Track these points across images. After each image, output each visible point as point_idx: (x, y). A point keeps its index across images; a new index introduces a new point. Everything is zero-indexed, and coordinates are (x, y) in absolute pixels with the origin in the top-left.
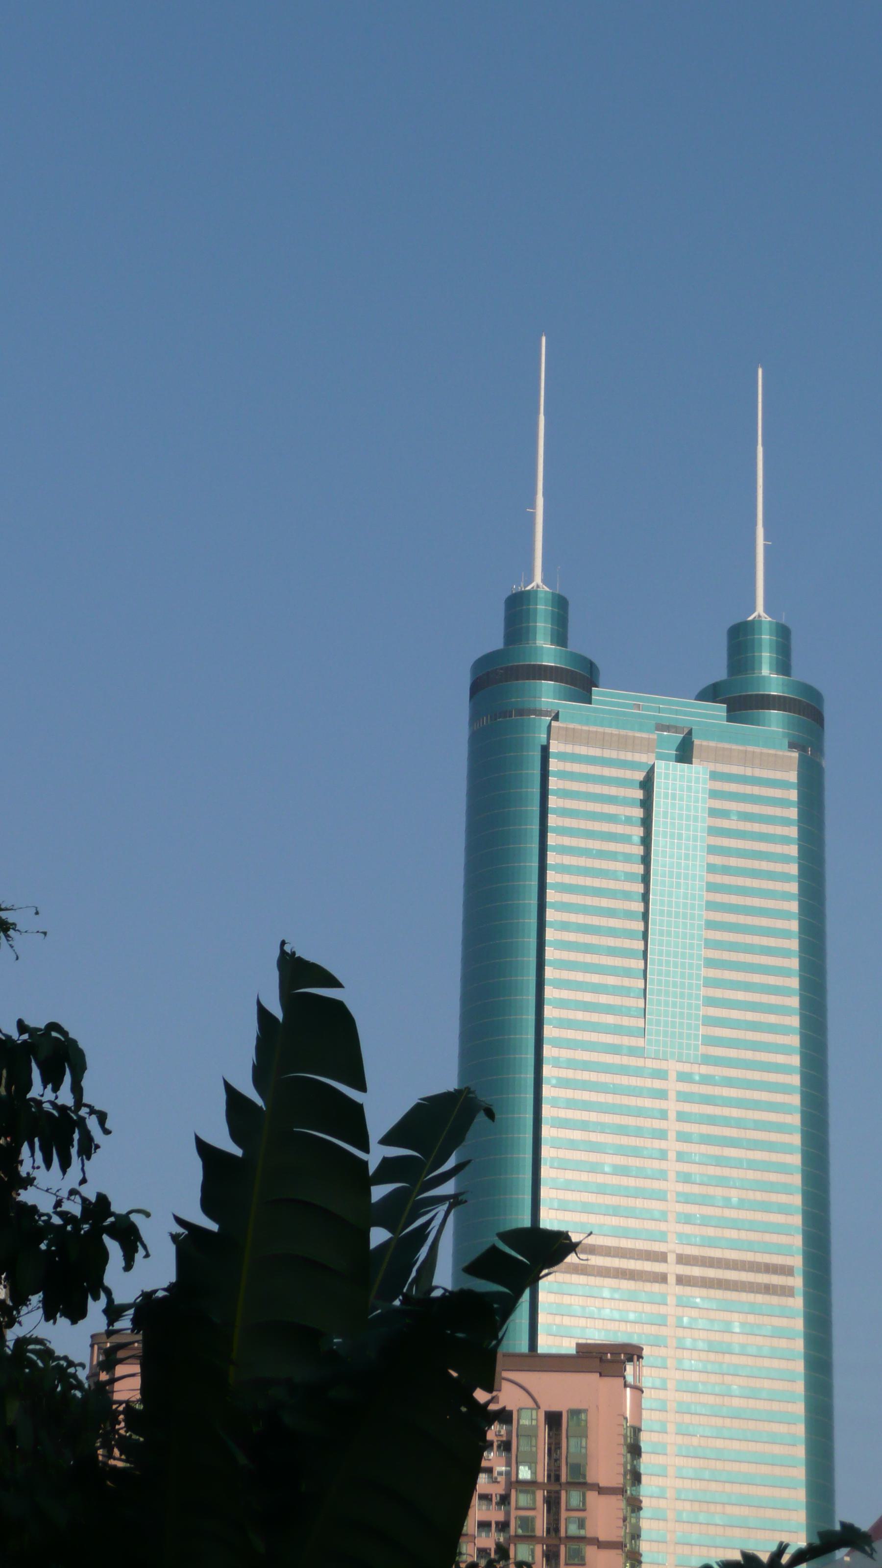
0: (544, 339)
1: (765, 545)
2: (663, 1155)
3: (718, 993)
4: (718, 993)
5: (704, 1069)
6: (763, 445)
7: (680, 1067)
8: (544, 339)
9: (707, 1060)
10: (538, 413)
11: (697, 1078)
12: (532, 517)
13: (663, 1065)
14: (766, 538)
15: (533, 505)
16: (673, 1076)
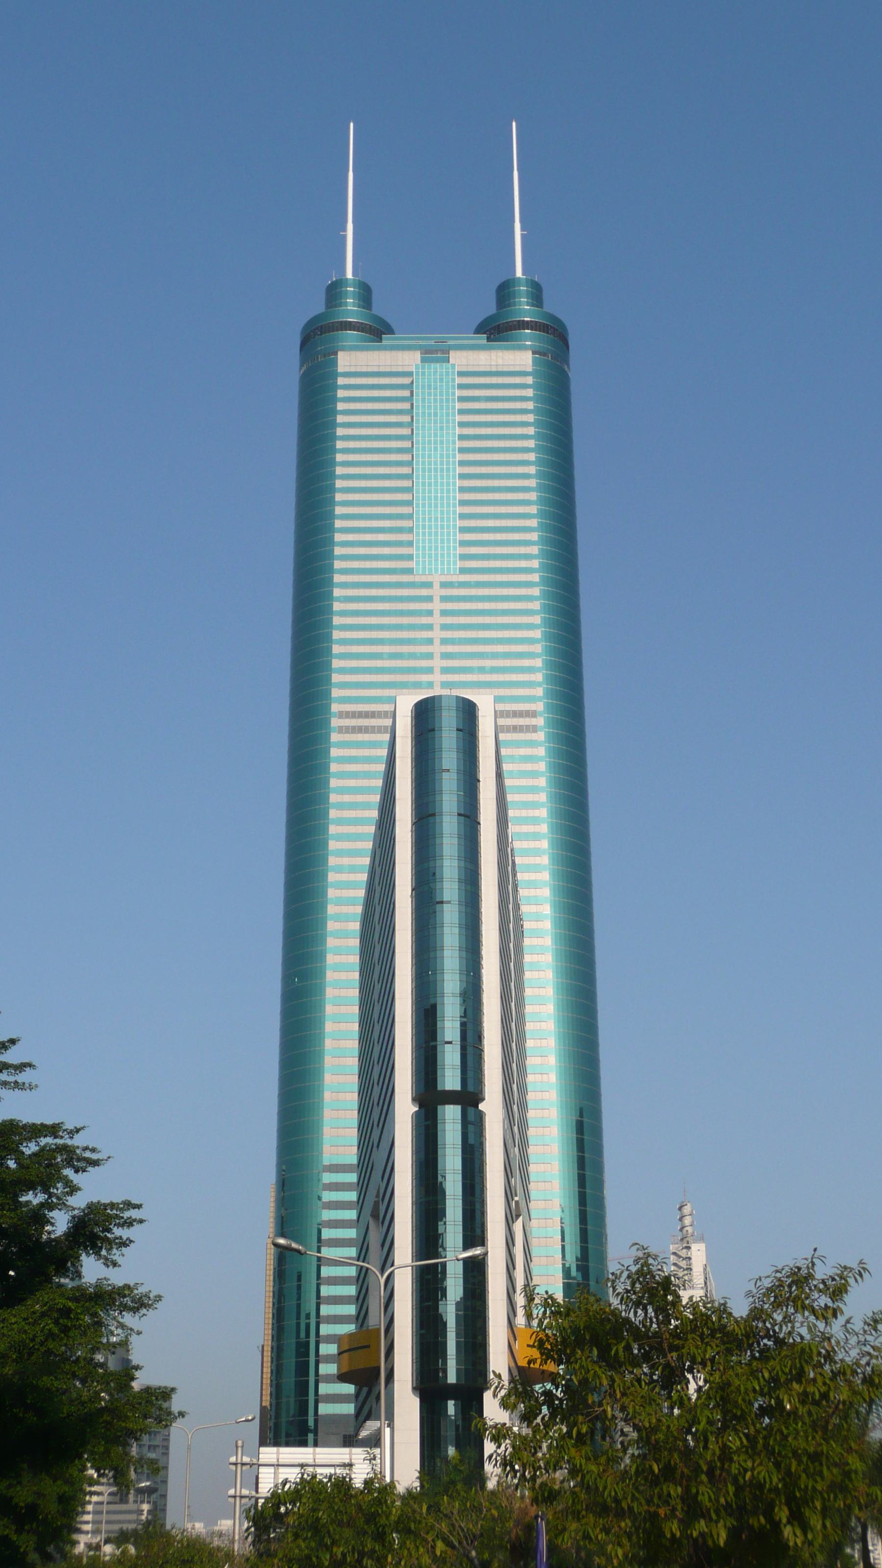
0: (352, 125)
1: (522, 235)
2: (430, 641)
3: (473, 523)
4: (473, 523)
5: (463, 578)
6: (518, 170)
7: (444, 579)
8: (352, 125)
9: (463, 571)
10: (348, 171)
11: (456, 585)
12: (344, 238)
13: (429, 579)
14: (522, 230)
15: (345, 229)
16: (436, 586)
